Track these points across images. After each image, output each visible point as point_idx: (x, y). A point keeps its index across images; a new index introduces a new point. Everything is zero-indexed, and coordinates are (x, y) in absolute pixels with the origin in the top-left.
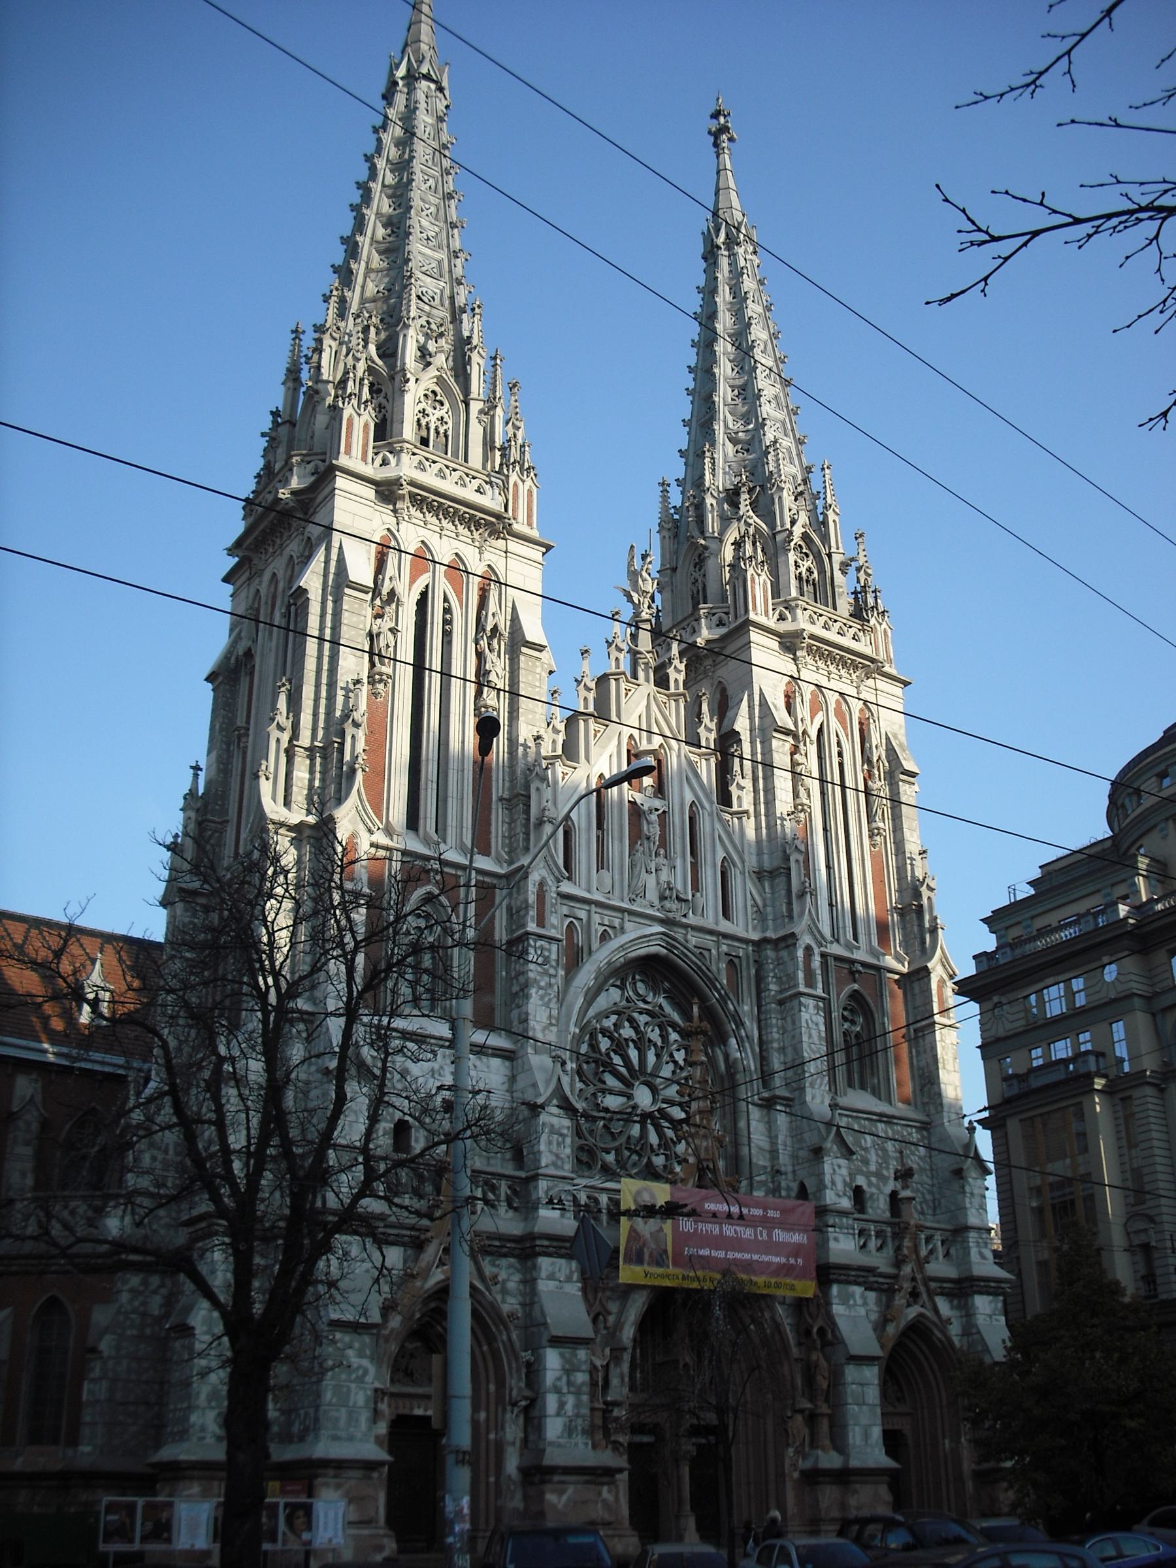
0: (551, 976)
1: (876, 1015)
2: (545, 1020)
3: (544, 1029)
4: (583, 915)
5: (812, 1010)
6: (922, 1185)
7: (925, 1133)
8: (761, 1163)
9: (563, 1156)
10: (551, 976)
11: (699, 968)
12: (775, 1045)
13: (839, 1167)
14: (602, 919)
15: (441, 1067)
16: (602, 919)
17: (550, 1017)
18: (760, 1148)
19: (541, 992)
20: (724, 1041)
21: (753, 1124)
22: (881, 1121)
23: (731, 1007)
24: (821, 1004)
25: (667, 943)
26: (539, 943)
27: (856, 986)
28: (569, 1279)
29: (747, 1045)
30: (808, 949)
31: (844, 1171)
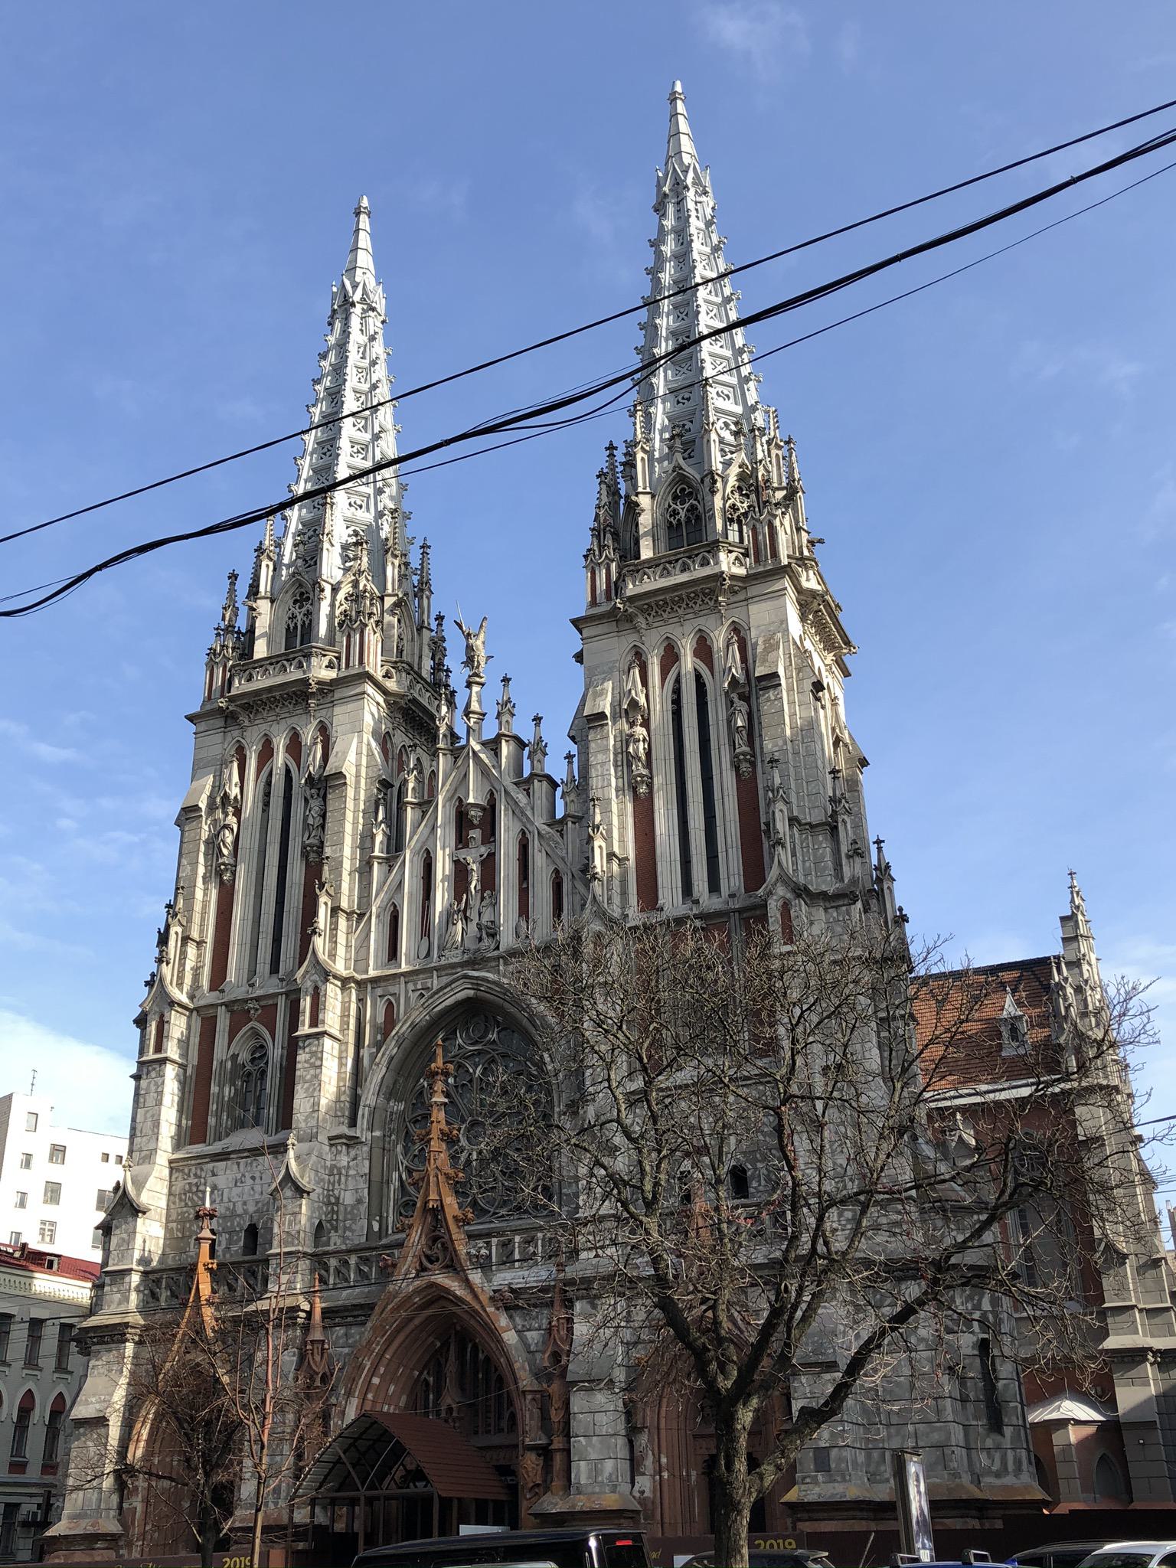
14: (415, 985)
15: (243, 1176)
19: (306, 1085)
25: (472, 984)
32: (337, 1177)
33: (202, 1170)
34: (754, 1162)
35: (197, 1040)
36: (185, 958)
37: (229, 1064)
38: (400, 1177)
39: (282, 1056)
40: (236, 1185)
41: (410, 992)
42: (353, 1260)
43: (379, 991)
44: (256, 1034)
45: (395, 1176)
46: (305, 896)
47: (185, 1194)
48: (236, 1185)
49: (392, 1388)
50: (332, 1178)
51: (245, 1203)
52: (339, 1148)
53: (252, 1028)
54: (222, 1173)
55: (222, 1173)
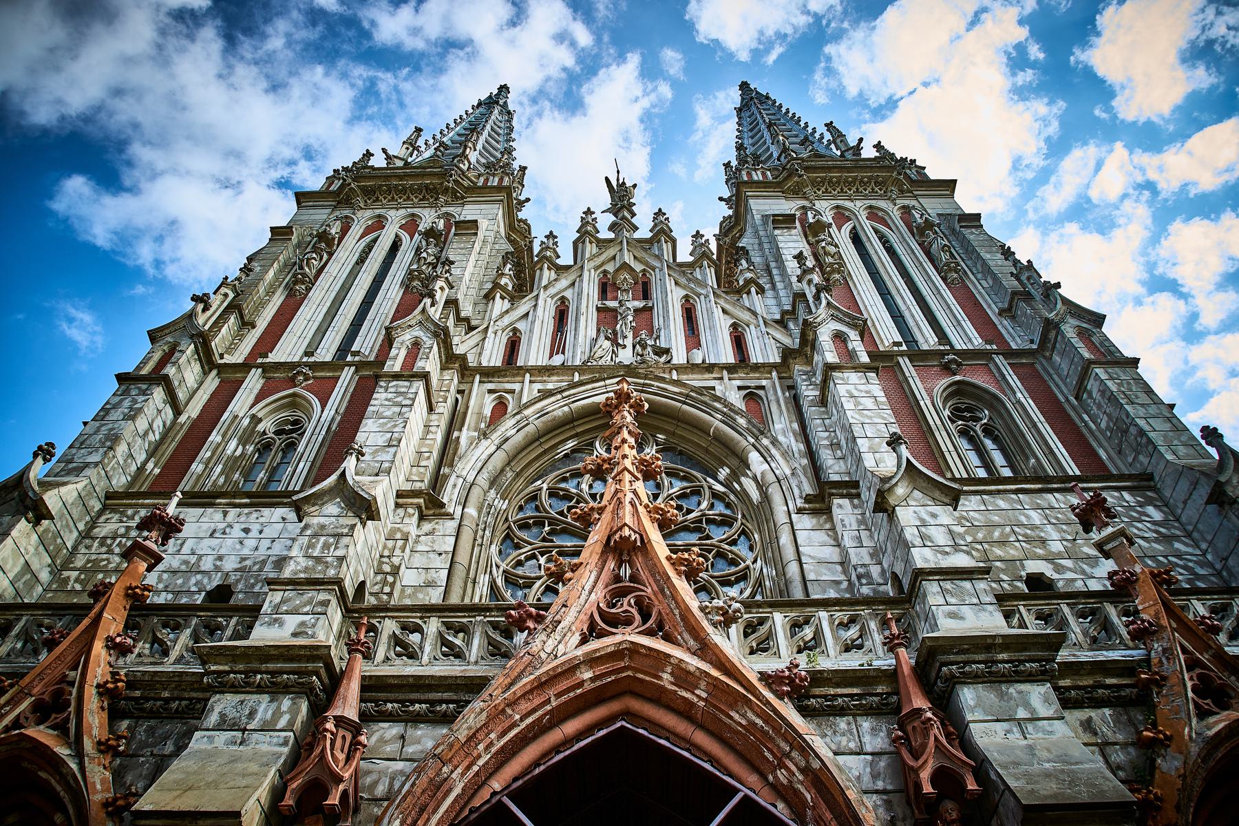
1: (1002, 396)
4: (517, 387)
6: (1179, 557)
7: (1149, 494)
9: (329, 559)
11: (687, 396)
12: (826, 442)
13: (934, 516)
19: (382, 421)
21: (801, 537)
22: (1051, 491)
23: (742, 421)
24: (874, 375)
26: (395, 383)
27: (958, 378)
28: (266, 728)
29: (774, 451)
30: (839, 337)
32: (400, 543)
35: (206, 397)
36: (224, 323)
37: (246, 422)
38: (493, 586)
39: (333, 419)
40: (211, 536)
42: (433, 626)
43: (491, 386)
44: (294, 402)
47: (114, 538)
48: (211, 536)
50: (390, 544)
51: (220, 558)
52: (410, 510)
53: (294, 395)
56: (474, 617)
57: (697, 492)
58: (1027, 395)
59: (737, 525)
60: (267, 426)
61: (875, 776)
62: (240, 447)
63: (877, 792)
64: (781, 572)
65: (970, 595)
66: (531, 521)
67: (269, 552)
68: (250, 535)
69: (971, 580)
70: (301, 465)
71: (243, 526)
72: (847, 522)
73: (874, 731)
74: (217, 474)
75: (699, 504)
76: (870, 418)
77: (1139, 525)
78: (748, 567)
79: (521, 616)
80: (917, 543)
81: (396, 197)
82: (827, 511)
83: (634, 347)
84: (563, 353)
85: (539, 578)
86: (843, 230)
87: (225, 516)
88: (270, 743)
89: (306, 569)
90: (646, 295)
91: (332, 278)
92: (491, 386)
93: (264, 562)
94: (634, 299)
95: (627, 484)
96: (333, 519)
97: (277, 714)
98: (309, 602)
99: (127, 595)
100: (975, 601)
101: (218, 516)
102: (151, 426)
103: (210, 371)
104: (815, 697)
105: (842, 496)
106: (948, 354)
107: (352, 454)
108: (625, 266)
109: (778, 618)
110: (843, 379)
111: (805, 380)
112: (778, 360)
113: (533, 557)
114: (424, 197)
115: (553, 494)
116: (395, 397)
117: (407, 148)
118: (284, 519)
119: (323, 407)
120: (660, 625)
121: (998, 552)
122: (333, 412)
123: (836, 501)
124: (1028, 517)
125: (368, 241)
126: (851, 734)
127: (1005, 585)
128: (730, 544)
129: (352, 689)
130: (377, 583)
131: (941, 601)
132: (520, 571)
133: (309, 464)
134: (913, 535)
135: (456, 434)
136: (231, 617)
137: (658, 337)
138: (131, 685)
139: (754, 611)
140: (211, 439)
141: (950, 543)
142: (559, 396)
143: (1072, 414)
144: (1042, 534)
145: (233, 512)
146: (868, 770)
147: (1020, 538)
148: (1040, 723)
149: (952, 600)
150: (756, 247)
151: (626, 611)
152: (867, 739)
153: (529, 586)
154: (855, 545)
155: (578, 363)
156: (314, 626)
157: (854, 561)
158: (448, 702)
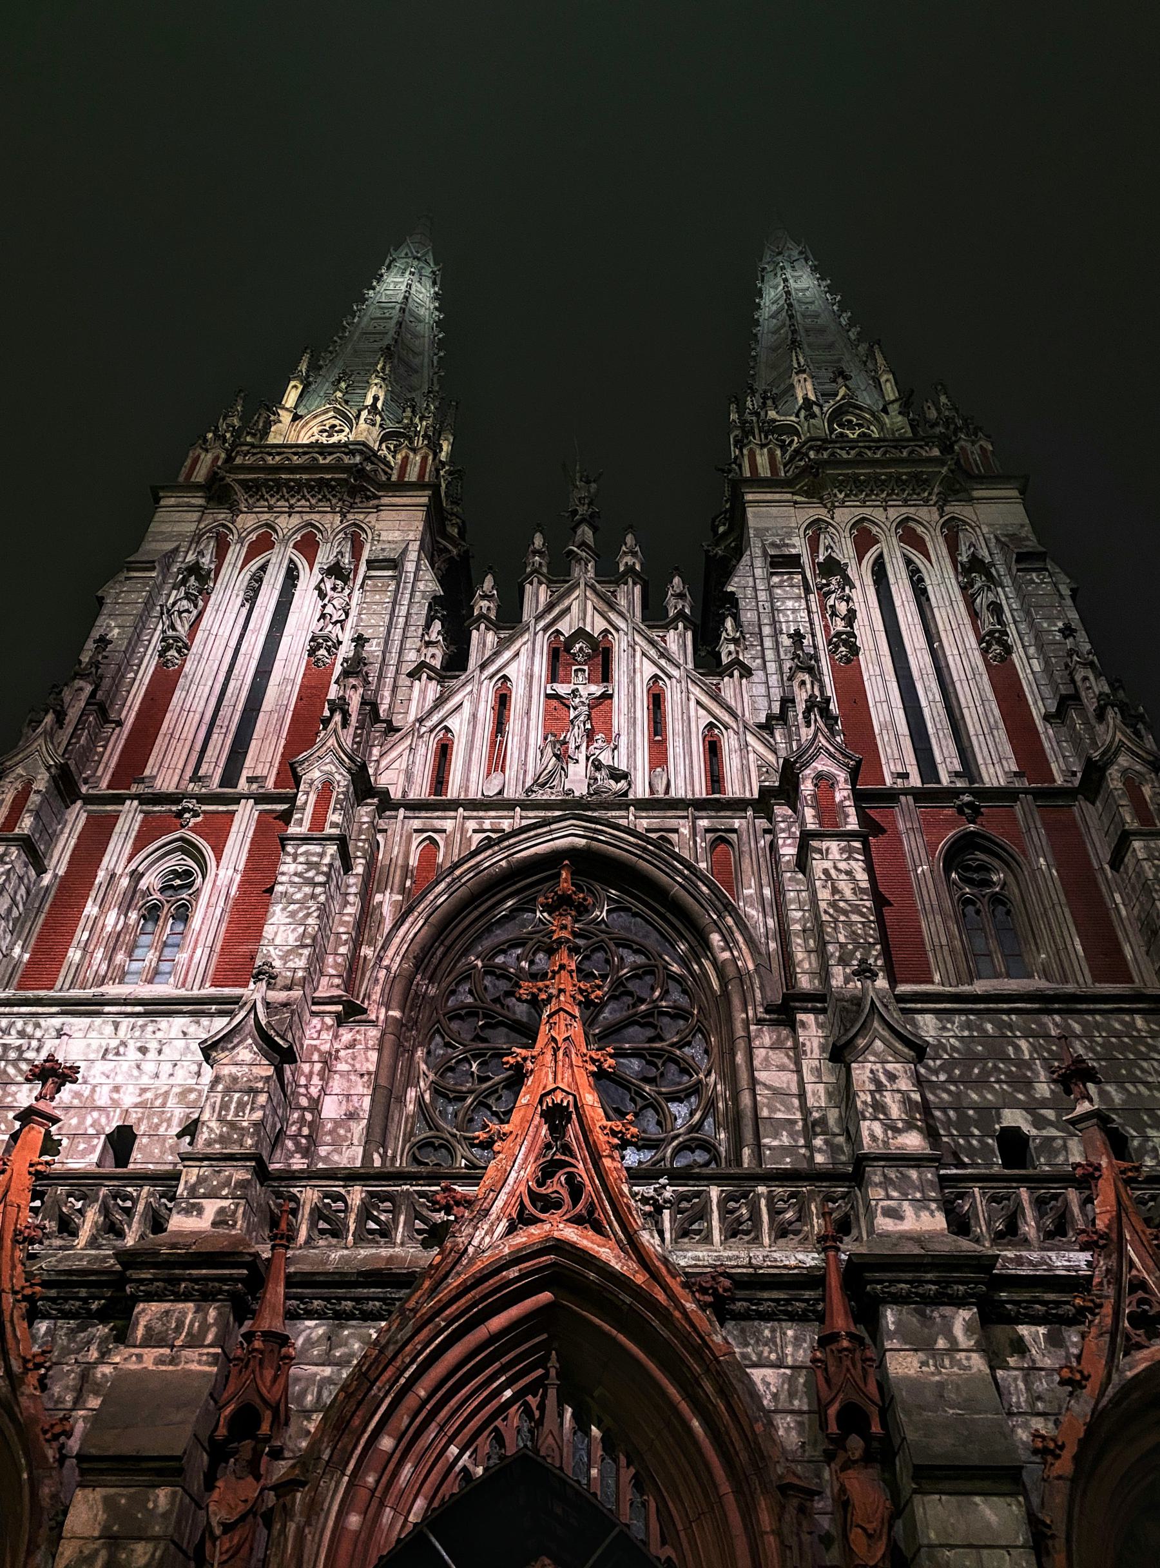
0: (316, 885)
1: (1021, 858)
2: (292, 939)
3: (284, 958)
5: (835, 853)
8: (779, 1115)
9: (245, 1124)
10: (316, 885)
11: (645, 849)
12: (797, 927)
15: (124, 1044)
16: (481, 824)
17: (303, 934)
18: (777, 1092)
19: (292, 907)
20: (707, 945)
21: (760, 1054)
22: (1050, 1012)
27: (972, 827)
28: (195, 1341)
30: (824, 781)
31: (904, 1084)
32: (318, 1067)
33: (37, 1026)
34: (1141, 1127)
37: (125, 882)
38: (420, 1100)
39: (232, 880)
40: (103, 1058)
41: (470, 833)
43: (417, 824)
45: (411, 1094)
46: (300, 698)
49: (408, 1469)
50: (306, 1067)
51: (117, 1089)
52: (329, 1021)
54: (81, 1034)
55: (81, 1034)
56: (400, 1185)
57: (650, 971)
58: (1051, 862)
59: (692, 1021)
60: (151, 880)
61: (792, 1395)
62: (122, 917)
63: (792, 1412)
64: (736, 1096)
65: (917, 1189)
66: (463, 1012)
67: (172, 1081)
68: (150, 1056)
69: (918, 1166)
70: (199, 951)
71: (139, 1044)
72: (808, 1048)
73: (797, 1341)
74: (98, 961)
75: (653, 989)
76: (845, 913)
77: (1145, 1064)
78: (700, 1081)
79: (448, 1203)
80: (868, 1115)
81: (287, 496)
82: (792, 1025)
83: (588, 758)
84: (503, 771)
85: (471, 1092)
86: (864, 562)
87: (116, 1029)
88: (199, 1362)
89: (222, 1139)
90: (606, 677)
91: (212, 638)
92: (417, 824)
93: (166, 1094)
94: (590, 681)
95: (563, 1028)
96: (246, 1069)
97: (205, 1327)
98: (227, 1183)
99: (30, 1173)
100: (918, 1195)
101: (109, 1029)
102: (13, 900)
103: (74, 802)
104: (740, 1300)
105: (806, 1011)
106: (964, 794)
107: (262, 980)
108: (581, 634)
109: (714, 1192)
110: (820, 851)
111: (783, 831)
112: (756, 796)
113: (466, 1059)
114: (324, 496)
115: (489, 971)
116: (307, 871)
117: (295, 387)
118: (185, 1034)
119: (218, 859)
120: (591, 1209)
121: (974, 1096)
122: (231, 871)
123: (801, 1017)
124: (1017, 1048)
125: (254, 569)
126: (775, 1344)
127: (975, 1142)
128: (680, 1048)
129: (277, 1292)
130: (294, 1123)
131: (882, 1194)
132: (450, 1080)
133: (207, 951)
134: (865, 1103)
135: (378, 897)
136: (141, 1186)
137: (616, 747)
138: (45, 1284)
139: (692, 1182)
140: (85, 912)
141: (904, 1116)
142: (496, 848)
143: (1104, 888)
144: (1029, 1074)
145: (126, 1023)
146: (786, 1386)
147: (1003, 1077)
148: (961, 1356)
149: (895, 1194)
150: (749, 592)
151: (556, 1192)
152: (789, 1350)
153: (464, 1099)
154: (814, 1079)
155: (520, 795)
156: (235, 1212)
157: (811, 1102)
158: (373, 1299)
